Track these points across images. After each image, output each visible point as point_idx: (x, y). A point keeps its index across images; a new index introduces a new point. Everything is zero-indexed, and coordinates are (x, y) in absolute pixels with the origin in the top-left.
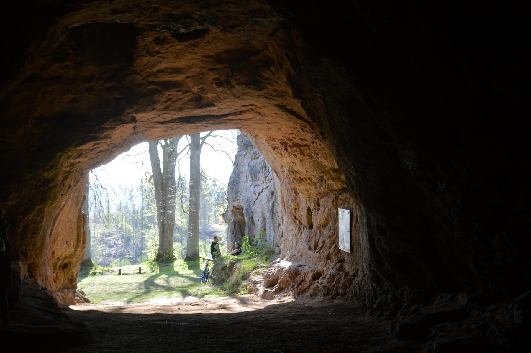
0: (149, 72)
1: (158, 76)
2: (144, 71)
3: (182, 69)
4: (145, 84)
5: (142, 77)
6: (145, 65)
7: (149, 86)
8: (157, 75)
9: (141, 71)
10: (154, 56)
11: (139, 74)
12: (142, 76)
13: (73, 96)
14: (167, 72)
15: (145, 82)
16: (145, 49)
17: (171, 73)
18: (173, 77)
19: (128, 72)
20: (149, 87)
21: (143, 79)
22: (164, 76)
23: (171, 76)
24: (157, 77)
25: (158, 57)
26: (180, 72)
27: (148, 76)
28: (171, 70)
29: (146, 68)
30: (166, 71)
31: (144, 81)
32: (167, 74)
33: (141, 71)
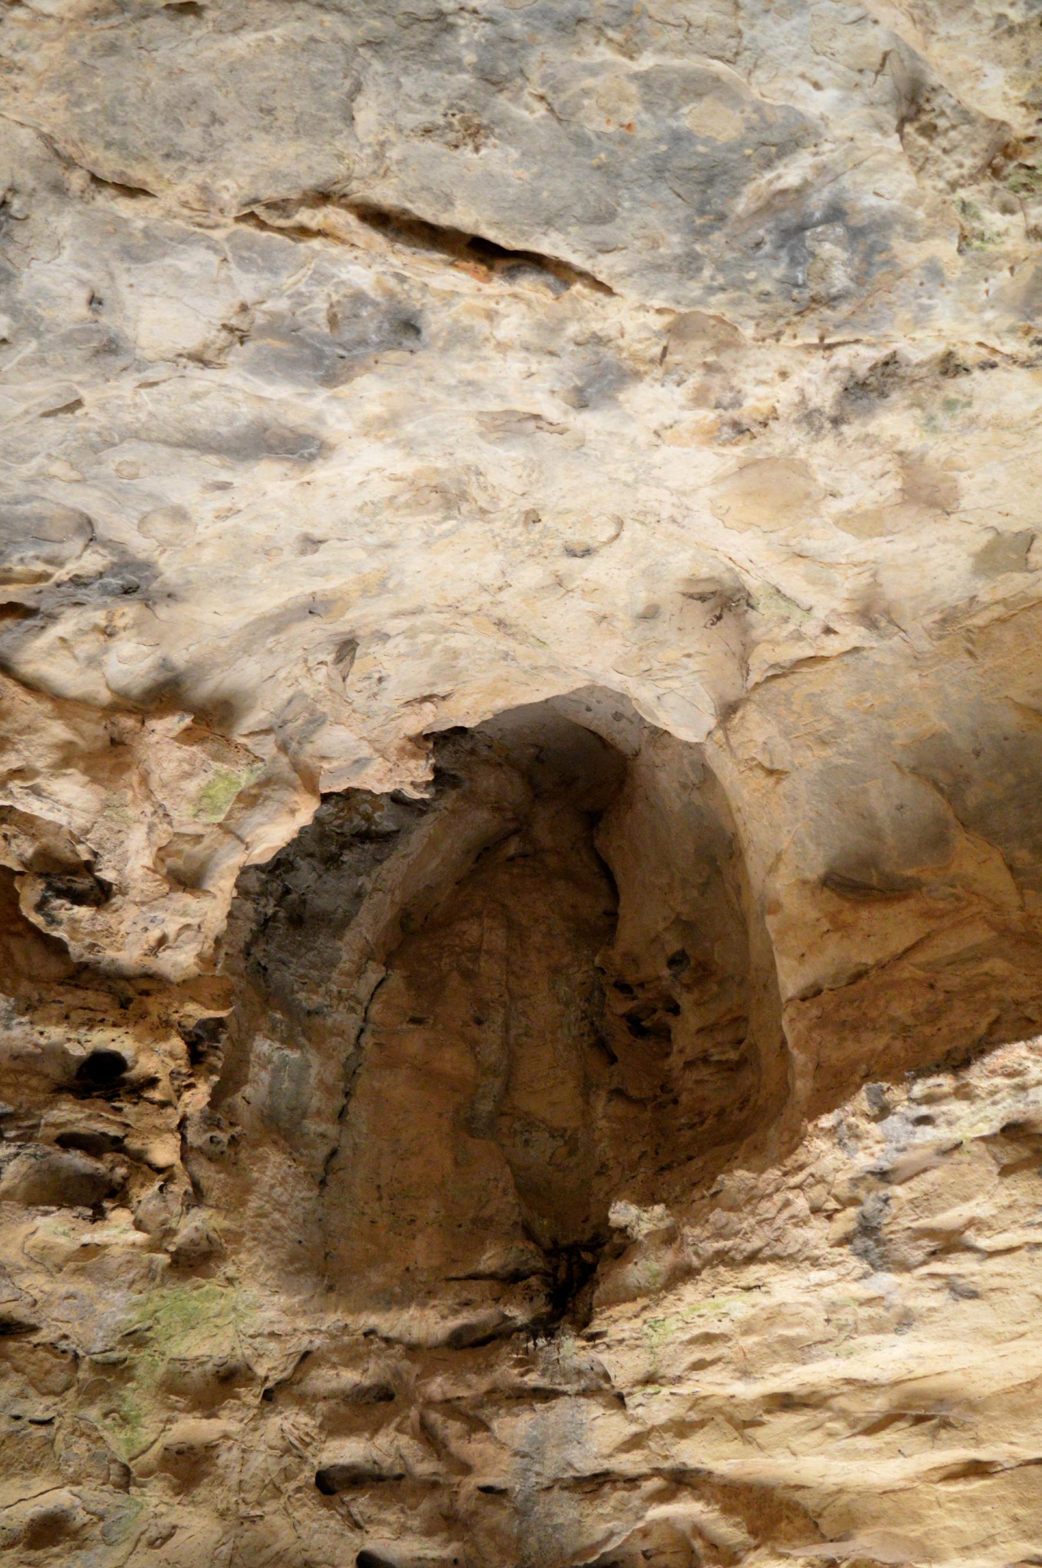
0: (696, 1401)
1: (758, 1433)
2: (678, 1380)
3: (973, 1406)
4: (632, 1482)
5: (635, 1428)
6: (708, 1339)
7: (662, 1496)
8: (757, 1424)
9: (650, 1380)
10: (905, 1267)
11: (619, 1401)
12: (633, 1420)
13: (62, 1498)
14: (843, 1414)
15: (645, 1469)
16: (855, 1202)
17: (873, 1428)
18: (879, 1451)
19: (533, 1380)
20: (658, 1512)
21: (635, 1442)
22: (816, 1436)
23: (864, 1442)
24: (749, 1441)
25: (933, 1275)
26: (946, 1424)
27: (682, 1429)
28: (880, 1404)
29: (700, 1365)
30: (841, 1402)
31: (629, 1463)
32: (837, 1426)
33: (650, 1380)
